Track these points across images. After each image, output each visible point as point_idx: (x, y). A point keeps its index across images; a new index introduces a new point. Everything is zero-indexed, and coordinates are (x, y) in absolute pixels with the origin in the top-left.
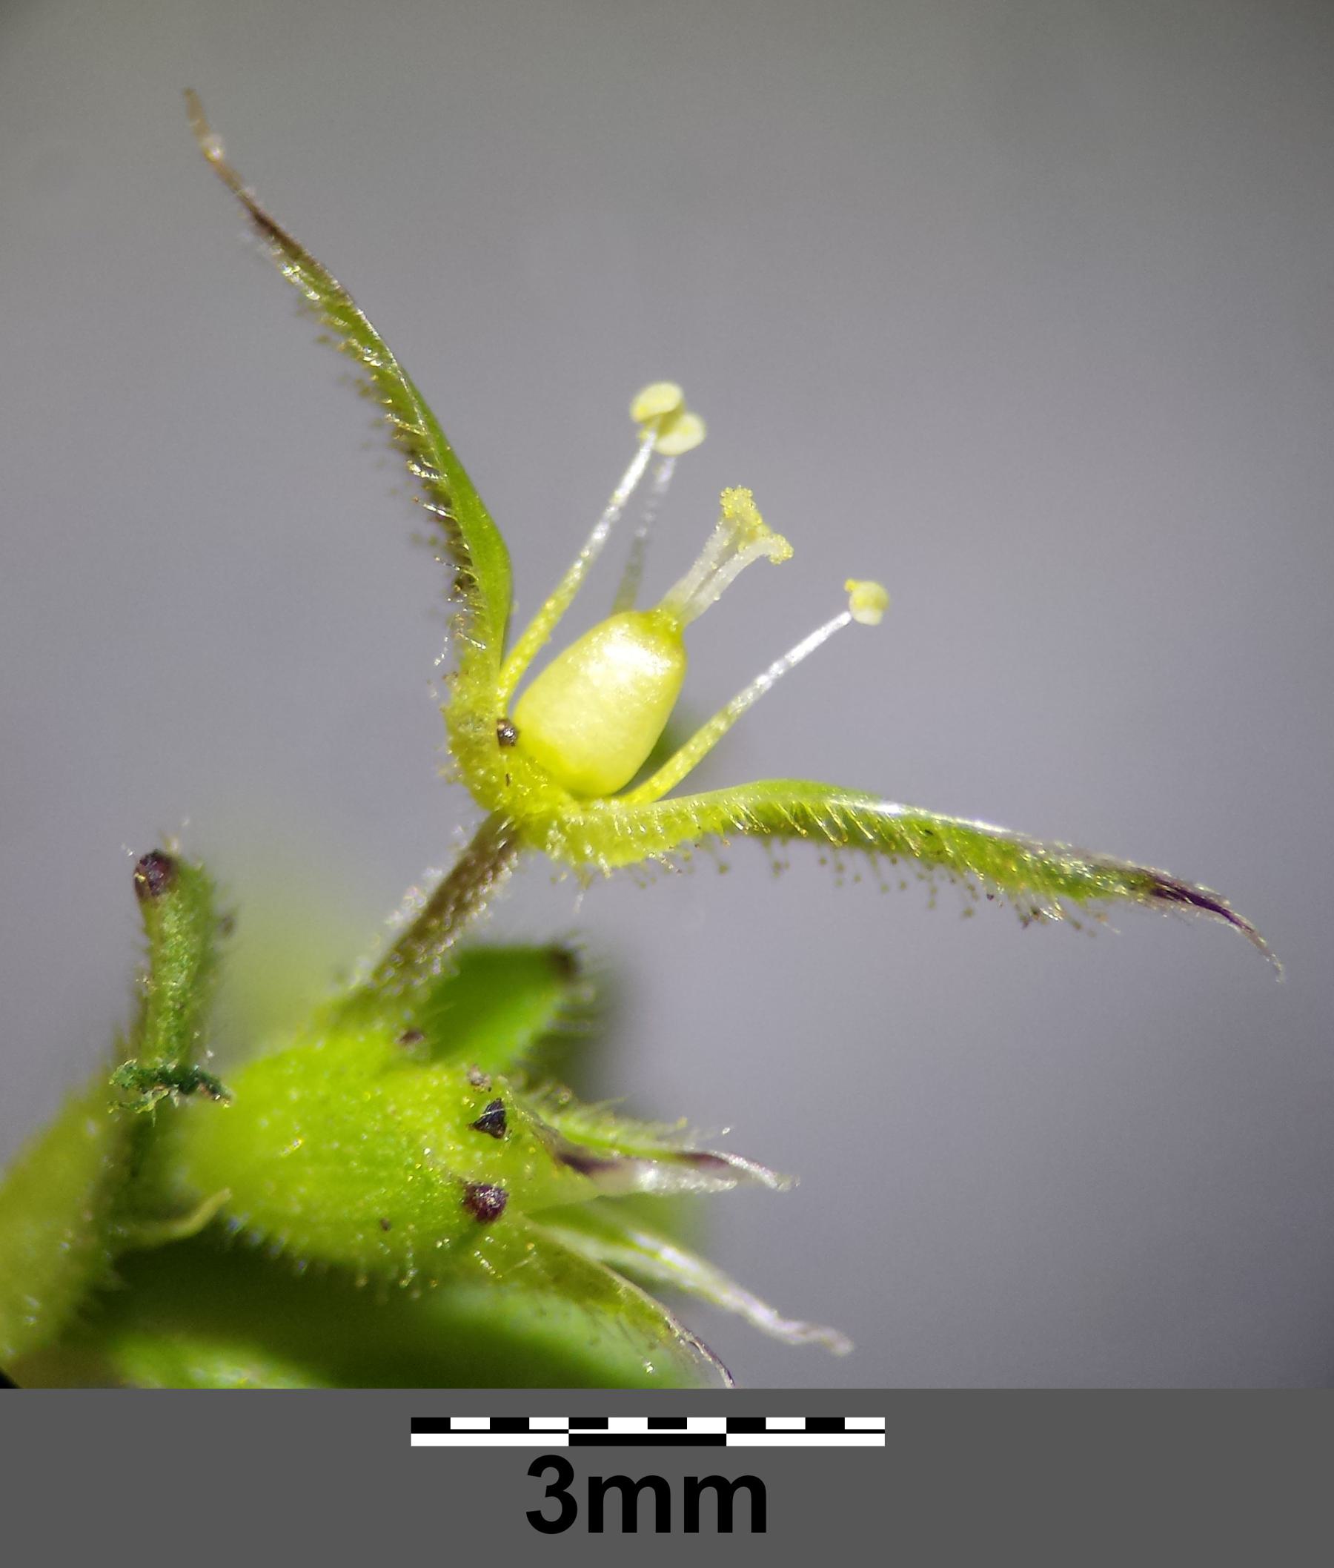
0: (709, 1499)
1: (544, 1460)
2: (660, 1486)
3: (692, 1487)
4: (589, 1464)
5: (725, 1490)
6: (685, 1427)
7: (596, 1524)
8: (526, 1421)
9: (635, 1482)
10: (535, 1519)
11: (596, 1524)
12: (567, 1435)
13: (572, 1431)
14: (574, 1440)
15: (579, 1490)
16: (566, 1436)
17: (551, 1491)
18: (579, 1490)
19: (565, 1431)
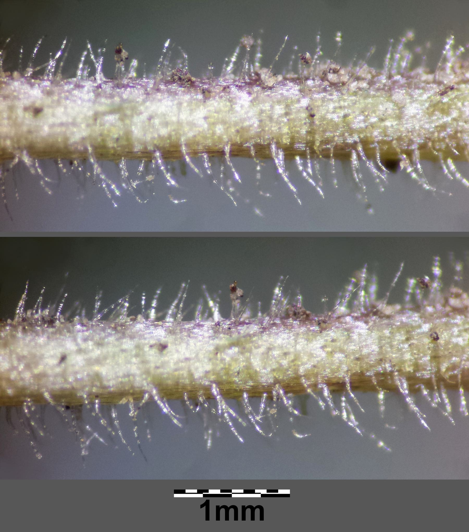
0: (248, 511)
3: (244, 508)
5: (227, 509)
8: (185, 490)
9: (254, 507)
13: (231, 493)
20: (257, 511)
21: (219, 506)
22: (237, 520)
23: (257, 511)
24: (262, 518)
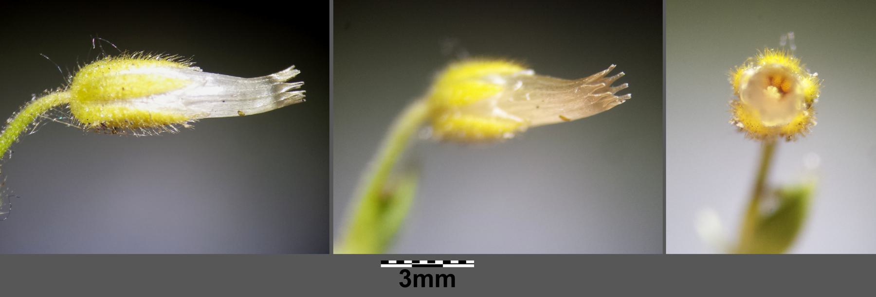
0: (442, 279)
1: (404, 271)
2: (430, 276)
3: (438, 277)
5: (445, 277)
7: (415, 285)
8: (403, 261)
9: (425, 275)
10: (401, 284)
11: (415, 285)
14: (413, 266)
15: (412, 277)
17: (405, 278)
18: (412, 277)
22: (432, 286)
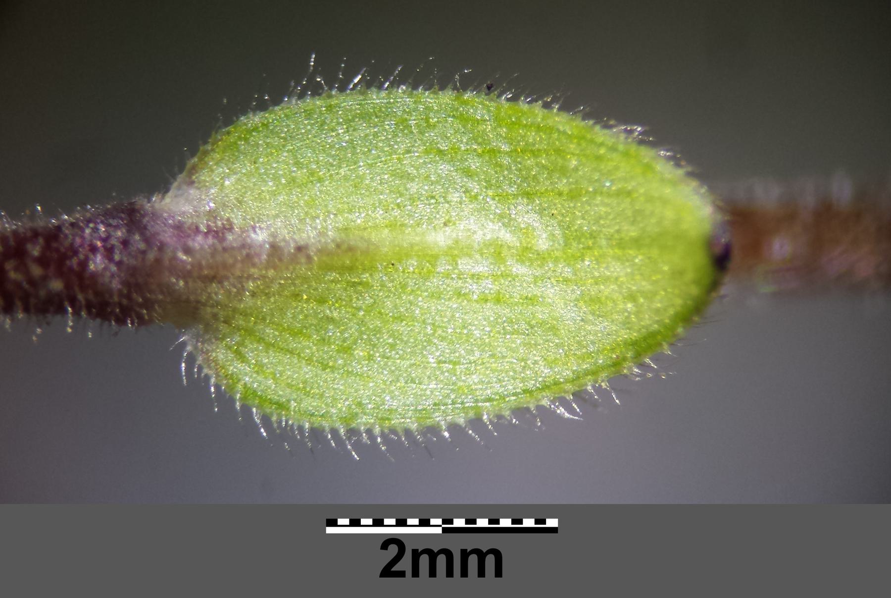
0: (473, 560)
2: (448, 554)
3: (465, 554)
4: (456, 544)
5: (433, 556)
6: (499, 524)
12: (441, 528)
13: (444, 526)
14: (444, 530)
16: (441, 528)
19: (440, 526)
20: (490, 560)
21: (418, 550)
23: (490, 560)
24: (499, 573)
